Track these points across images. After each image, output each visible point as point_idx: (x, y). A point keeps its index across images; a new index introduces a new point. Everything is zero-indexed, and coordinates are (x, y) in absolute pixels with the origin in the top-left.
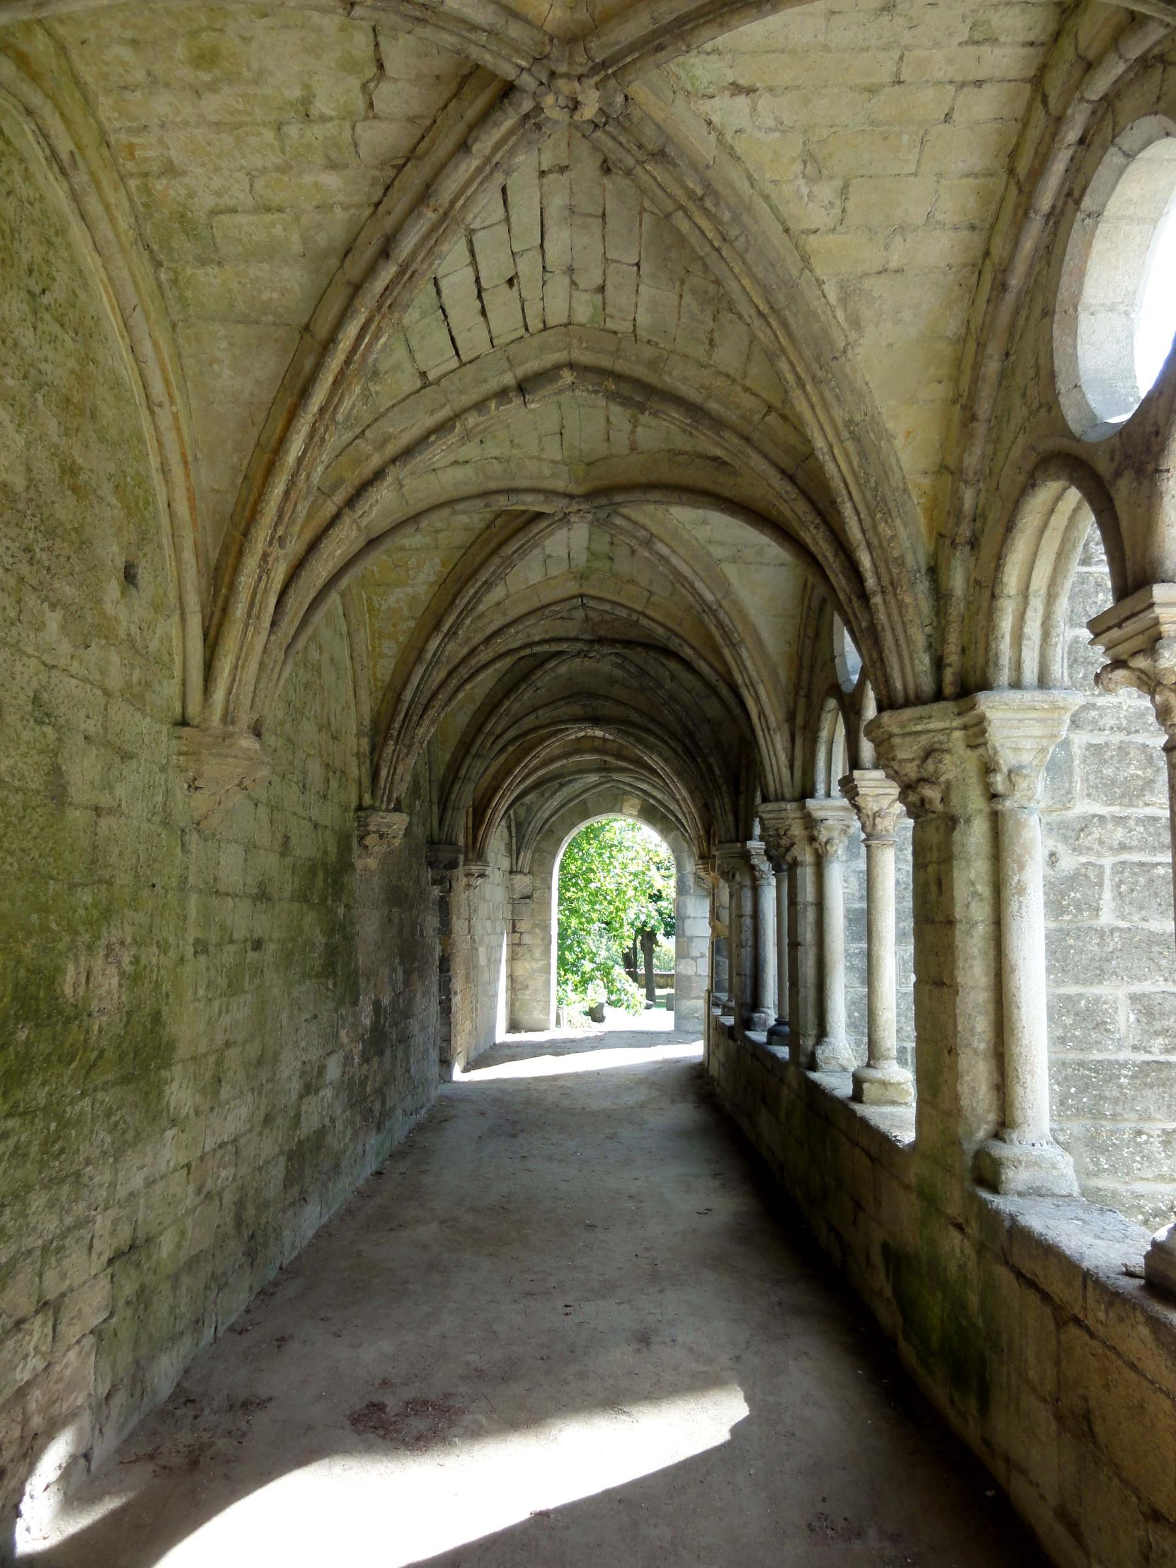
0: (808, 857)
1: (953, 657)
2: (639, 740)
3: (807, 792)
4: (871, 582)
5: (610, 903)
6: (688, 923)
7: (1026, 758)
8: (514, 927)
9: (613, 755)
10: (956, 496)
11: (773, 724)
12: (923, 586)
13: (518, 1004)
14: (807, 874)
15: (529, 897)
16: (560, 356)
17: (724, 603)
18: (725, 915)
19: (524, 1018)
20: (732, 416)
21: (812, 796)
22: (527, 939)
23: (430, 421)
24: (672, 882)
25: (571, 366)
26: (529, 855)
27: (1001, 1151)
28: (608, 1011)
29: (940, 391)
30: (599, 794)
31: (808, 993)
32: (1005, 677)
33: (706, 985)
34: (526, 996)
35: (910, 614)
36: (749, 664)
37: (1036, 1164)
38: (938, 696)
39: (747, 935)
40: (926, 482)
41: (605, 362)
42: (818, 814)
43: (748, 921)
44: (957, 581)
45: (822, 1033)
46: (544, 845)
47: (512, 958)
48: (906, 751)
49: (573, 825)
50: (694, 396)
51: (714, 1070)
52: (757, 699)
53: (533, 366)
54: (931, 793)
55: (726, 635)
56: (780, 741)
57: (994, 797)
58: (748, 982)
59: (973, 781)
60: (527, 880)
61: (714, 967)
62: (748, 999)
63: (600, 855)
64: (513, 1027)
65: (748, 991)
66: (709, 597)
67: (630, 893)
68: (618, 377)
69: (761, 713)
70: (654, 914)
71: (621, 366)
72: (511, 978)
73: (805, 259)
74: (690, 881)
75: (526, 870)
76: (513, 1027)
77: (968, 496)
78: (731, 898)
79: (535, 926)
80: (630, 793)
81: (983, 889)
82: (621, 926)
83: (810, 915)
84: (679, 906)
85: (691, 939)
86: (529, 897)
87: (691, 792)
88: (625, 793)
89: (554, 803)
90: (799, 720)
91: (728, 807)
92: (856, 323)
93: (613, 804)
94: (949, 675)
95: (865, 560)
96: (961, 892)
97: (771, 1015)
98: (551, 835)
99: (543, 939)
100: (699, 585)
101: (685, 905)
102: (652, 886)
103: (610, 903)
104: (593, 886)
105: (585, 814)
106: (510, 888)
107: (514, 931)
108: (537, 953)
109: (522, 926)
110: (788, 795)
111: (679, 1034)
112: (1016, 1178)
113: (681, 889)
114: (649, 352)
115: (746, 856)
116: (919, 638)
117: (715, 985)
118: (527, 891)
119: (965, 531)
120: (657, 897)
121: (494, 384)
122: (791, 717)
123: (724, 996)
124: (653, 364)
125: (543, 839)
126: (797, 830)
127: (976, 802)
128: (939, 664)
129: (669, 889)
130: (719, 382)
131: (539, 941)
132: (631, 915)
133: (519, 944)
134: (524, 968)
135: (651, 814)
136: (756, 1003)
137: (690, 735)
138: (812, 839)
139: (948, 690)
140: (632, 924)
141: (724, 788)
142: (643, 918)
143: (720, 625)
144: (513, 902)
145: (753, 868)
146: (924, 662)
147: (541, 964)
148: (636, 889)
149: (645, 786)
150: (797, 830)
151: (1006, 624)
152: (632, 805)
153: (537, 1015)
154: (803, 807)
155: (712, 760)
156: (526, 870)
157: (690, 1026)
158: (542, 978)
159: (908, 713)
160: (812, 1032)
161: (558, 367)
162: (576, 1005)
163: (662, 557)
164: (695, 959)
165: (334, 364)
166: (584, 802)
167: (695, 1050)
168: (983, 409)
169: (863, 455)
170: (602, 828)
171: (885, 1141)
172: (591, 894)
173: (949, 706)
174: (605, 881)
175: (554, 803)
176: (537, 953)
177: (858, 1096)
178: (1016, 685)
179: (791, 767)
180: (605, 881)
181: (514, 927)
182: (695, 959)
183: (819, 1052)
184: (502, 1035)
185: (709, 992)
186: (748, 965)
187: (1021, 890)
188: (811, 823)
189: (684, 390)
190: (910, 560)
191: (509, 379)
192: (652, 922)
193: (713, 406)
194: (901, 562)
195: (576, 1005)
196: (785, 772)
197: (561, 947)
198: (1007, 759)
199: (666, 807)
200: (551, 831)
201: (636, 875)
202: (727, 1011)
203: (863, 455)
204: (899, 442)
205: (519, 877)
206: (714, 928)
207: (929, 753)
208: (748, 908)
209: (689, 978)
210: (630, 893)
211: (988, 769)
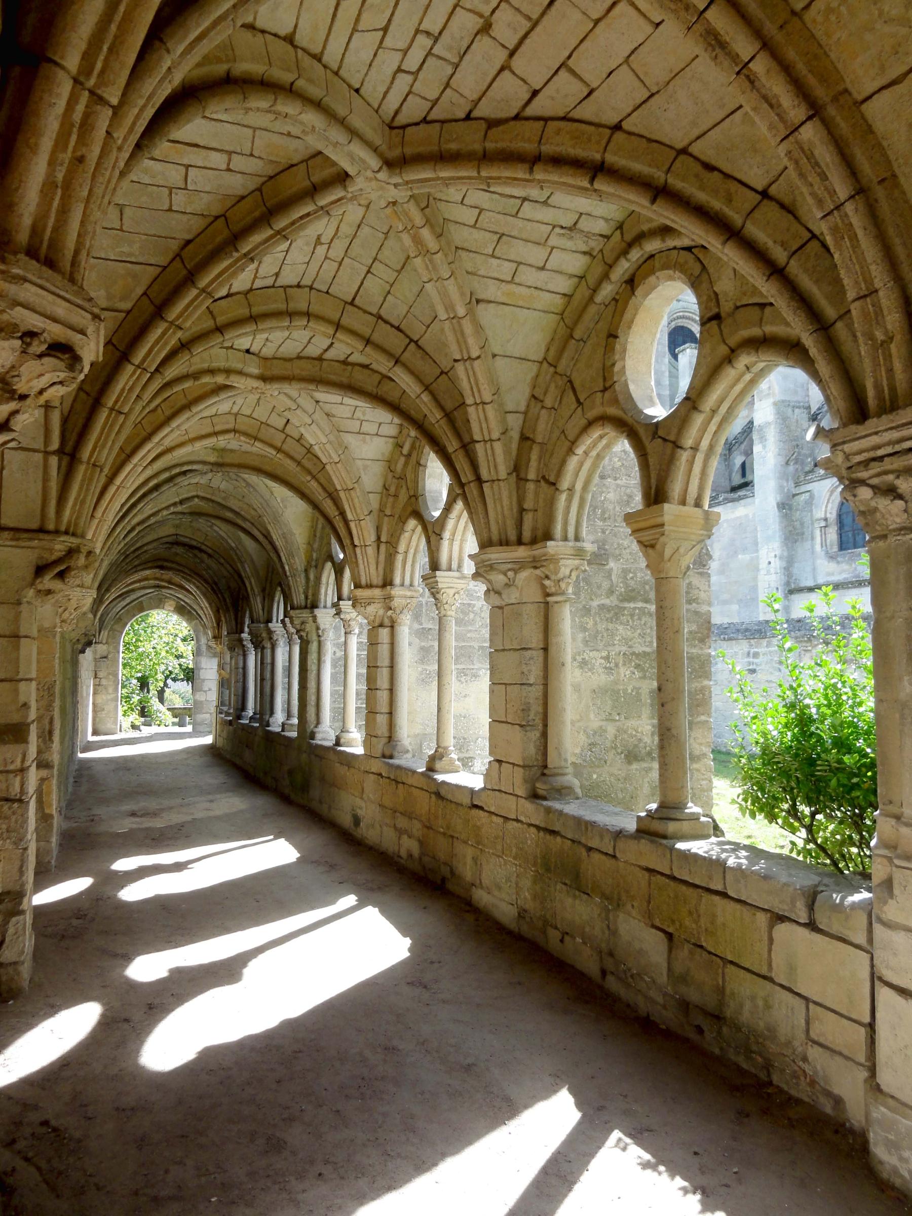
0: (268, 645)
1: (310, 597)
2: (183, 577)
3: (269, 620)
4: (288, 574)
5: (150, 660)
6: (202, 672)
7: (327, 626)
8: (96, 674)
9: (166, 581)
10: (312, 556)
11: (256, 593)
12: (303, 575)
13: (98, 720)
14: (268, 652)
15: (105, 657)
16: (194, 493)
17: (240, 547)
18: (228, 667)
19: (101, 727)
20: (249, 517)
21: (271, 622)
22: (104, 682)
23: (150, 512)
24: (190, 648)
25: (198, 496)
26: (106, 633)
27: (316, 730)
28: (142, 727)
29: (309, 524)
30: (151, 598)
31: (267, 699)
32: (322, 605)
33: (215, 704)
34: (102, 715)
35: (299, 583)
36: (248, 569)
37: (324, 732)
38: (306, 607)
39: (241, 676)
40: (305, 546)
41: (209, 496)
42: (273, 629)
43: (241, 670)
44: (312, 576)
45: (272, 713)
46: (116, 627)
47: (94, 694)
48: (297, 622)
49: (134, 616)
50: (237, 510)
51: (220, 744)
52: (251, 583)
53: (185, 496)
54: (304, 634)
55: (239, 559)
56: (259, 599)
57: (319, 636)
58: (240, 698)
59: (314, 631)
60: (105, 647)
61: (221, 694)
62: (240, 707)
63: (145, 631)
64: (95, 733)
65: (240, 702)
66: (233, 545)
67: (163, 654)
68: (213, 501)
69: (252, 589)
70: (178, 666)
71: (213, 498)
72: (94, 704)
73: (272, 493)
74: (204, 648)
75: (104, 642)
76: (95, 733)
77: (315, 555)
78: (231, 658)
79: (109, 674)
80: (169, 598)
81: (315, 661)
82: (156, 674)
83: (269, 667)
84: (196, 663)
85: (204, 680)
86: (105, 657)
87: (210, 604)
88: (167, 597)
89: (124, 603)
90: (267, 592)
91: (233, 617)
92: (286, 507)
93: (159, 604)
94: (309, 601)
95: (287, 568)
96: (309, 663)
97: (250, 712)
98: (122, 620)
99: (114, 681)
100: (230, 541)
101: (200, 662)
102: (177, 650)
103: (150, 660)
104: (140, 650)
105: (141, 609)
106: (95, 652)
107: (96, 677)
108: (110, 690)
109: (100, 674)
110: (261, 619)
111: (195, 733)
112: (319, 736)
113: (197, 653)
114: (223, 495)
115: (241, 640)
116: (301, 590)
117: (221, 703)
118: (105, 654)
119: (313, 563)
120: (178, 657)
121: (172, 501)
122: (264, 590)
123: (225, 709)
124: (224, 499)
125: (115, 623)
126: (264, 635)
127: (315, 637)
128: (306, 598)
129: (187, 649)
130: (245, 506)
131: (111, 683)
132: (163, 667)
133: (99, 685)
134: (101, 699)
135: (182, 610)
136: (243, 707)
137: (216, 584)
138: (271, 638)
139: (309, 606)
140: (163, 673)
141: (231, 609)
142: (170, 669)
143: (236, 554)
144: (95, 660)
145: (244, 646)
146: (303, 597)
147: (112, 696)
148: (167, 652)
149: (180, 596)
150: (264, 635)
151: (323, 591)
152: (170, 604)
153: (110, 726)
154: (267, 626)
155: (226, 596)
156: (104, 642)
157: (201, 728)
158: (113, 705)
159: (298, 611)
160: (268, 713)
161: (193, 497)
162: (126, 722)
163: (215, 531)
164: (205, 692)
165: (135, 511)
166: (141, 602)
167: (208, 740)
168: (318, 535)
169: (286, 542)
170: (147, 615)
171: (289, 739)
172: (139, 654)
173: (308, 611)
174: (146, 647)
175: (124, 603)
176: (110, 690)
177: (283, 730)
178: (325, 607)
179: (263, 610)
180: (146, 647)
181: (96, 674)
182: (205, 692)
183: (271, 720)
184: (91, 738)
185: (217, 707)
186: (240, 691)
187: (324, 662)
188: (270, 632)
189: (234, 507)
190: (299, 568)
191: (177, 500)
192: (176, 671)
193: (243, 513)
194: (296, 569)
195: (126, 722)
196: (261, 612)
197: (123, 687)
198: (322, 627)
199: (191, 607)
200: (120, 619)
201: (168, 644)
202: (228, 714)
203: (286, 542)
204: (297, 536)
205: (100, 645)
206: (220, 675)
207: (303, 623)
208: (241, 665)
209: (201, 702)
210: (163, 654)
211: (318, 628)
